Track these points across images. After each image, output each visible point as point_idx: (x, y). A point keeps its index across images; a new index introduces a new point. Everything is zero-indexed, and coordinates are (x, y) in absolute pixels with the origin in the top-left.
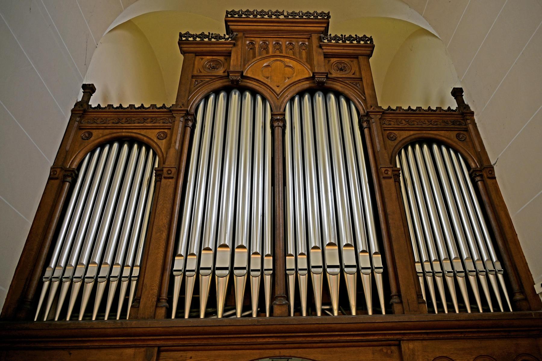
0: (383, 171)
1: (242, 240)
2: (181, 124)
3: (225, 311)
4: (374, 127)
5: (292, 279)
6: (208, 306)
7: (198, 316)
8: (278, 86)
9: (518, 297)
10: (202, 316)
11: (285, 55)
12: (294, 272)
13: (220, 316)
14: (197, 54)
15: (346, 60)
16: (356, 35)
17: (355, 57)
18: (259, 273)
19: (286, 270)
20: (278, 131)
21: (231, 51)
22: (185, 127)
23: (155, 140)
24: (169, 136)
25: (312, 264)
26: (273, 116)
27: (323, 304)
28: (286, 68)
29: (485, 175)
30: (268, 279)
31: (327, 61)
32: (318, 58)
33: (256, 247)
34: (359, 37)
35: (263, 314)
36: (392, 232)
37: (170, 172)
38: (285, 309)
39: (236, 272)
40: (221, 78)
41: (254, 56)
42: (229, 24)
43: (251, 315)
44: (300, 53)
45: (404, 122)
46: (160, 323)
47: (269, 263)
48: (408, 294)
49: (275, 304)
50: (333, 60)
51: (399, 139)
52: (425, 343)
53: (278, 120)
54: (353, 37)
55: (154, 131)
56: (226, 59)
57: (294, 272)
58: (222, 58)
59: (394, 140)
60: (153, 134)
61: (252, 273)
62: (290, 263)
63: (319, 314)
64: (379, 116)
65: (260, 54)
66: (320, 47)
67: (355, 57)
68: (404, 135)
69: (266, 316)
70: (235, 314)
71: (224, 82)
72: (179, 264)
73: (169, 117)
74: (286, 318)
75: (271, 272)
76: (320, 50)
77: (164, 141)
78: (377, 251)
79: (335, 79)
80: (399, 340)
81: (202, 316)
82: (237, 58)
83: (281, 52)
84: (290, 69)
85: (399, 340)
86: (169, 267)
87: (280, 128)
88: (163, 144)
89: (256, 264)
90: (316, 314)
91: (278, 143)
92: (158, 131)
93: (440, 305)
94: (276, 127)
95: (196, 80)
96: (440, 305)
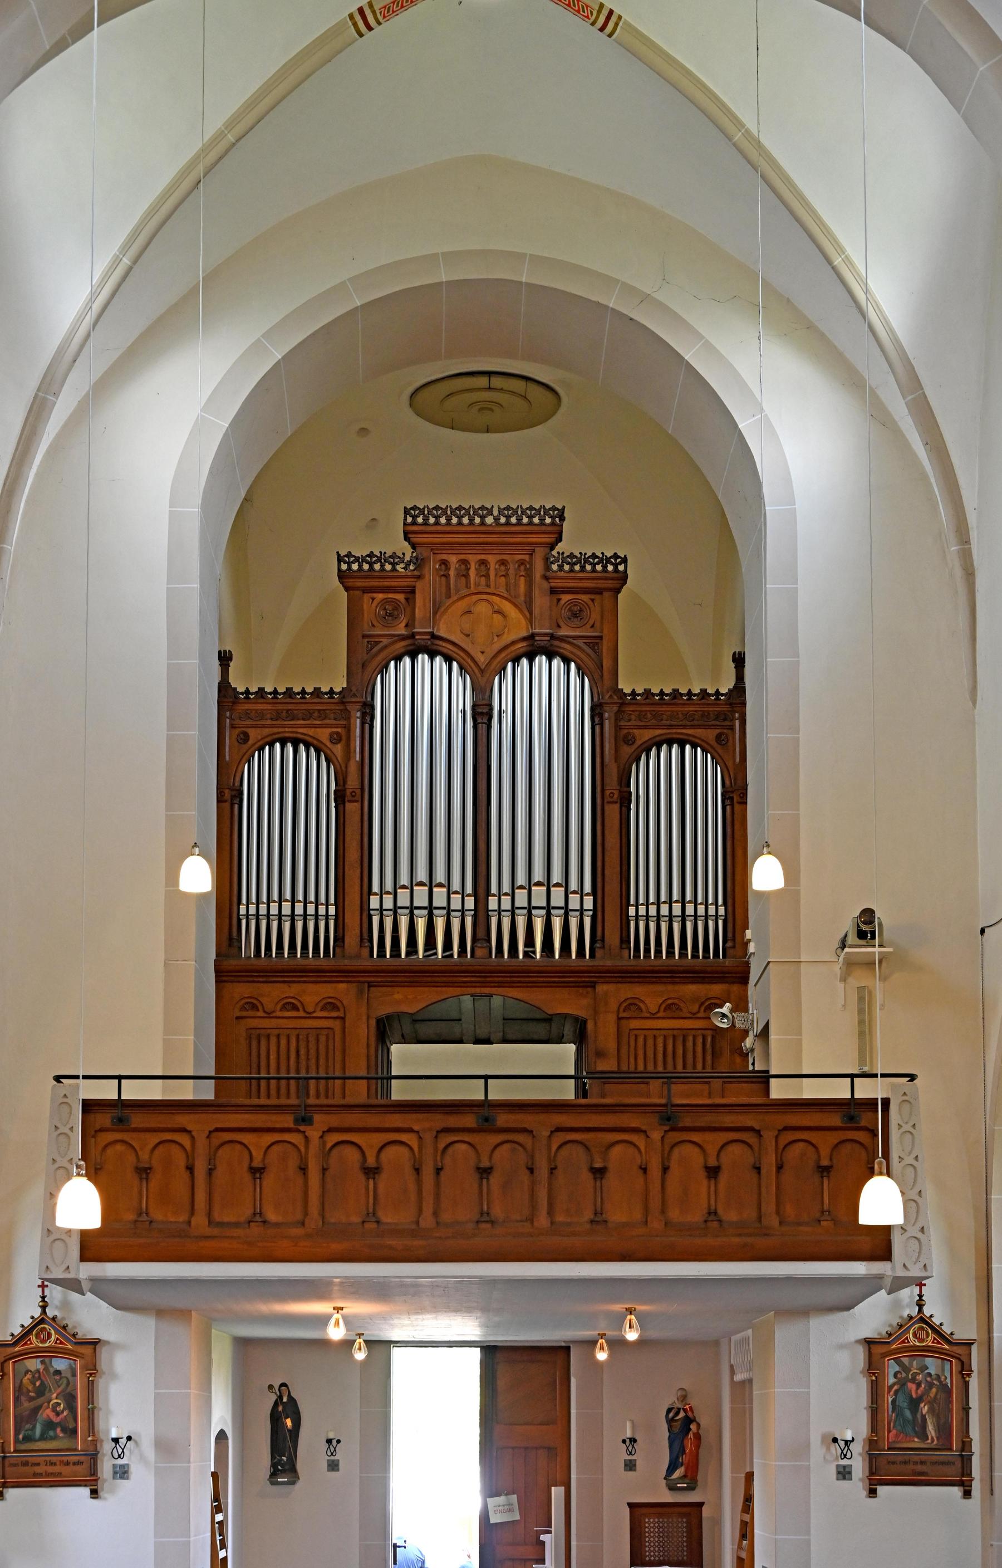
0: (608, 794)
1: (440, 877)
2: (358, 721)
3: (425, 950)
4: (607, 723)
5: (494, 921)
6: (408, 945)
7: (399, 956)
8: (483, 652)
9: (729, 944)
10: (403, 956)
11: (495, 592)
12: (496, 913)
13: (421, 957)
14: (365, 590)
15: (585, 598)
16: (603, 553)
17: (599, 592)
18: (459, 914)
19: (488, 910)
20: (482, 729)
21: (415, 587)
22: (363, 724)
23: (328, 744)
24: (344, 738)
25: (517, 905)
26: (476, 708)
27: (526, 945)
28: (495, 615)
29: (735, 800)
30: (469, 921)
31: (555, 601)
32: (541, 601)
33: (456, 885)
34: (606, 556)
35: (464, 955)
36: (607, 872)
37: (353, 794)
38: (486, 951)
39: (435, 912)
40: (403, 638)
41: (449, 596)
42: (410, 536)
43: (452, 956)
44: (516, 585)
45: (649, 715)
46: (365, 963)
47: (470, 903)
48: (612, 938)
49: (476, 946)
50: (565, 598)
51: (638, 743)
52: (620, 985)
53: (482, 713)
54: (597, 557)
55: (324, 730)
56: (407, 599)
57: (496, 913)
58: (400, 597)
59: (631, 744)
60: (323, 735)
61: (453, 914)
62: (493, 903)
63: (521, 956)
64: (615, 708)
65: (457, 591)
66: (546, 578)
67: (599, 592)
68: (647, 735)
69: (467, 956)
70: (436, 954)
71: (407, 646)
72: (374, 902)
73: (341, 710)
74: (487, 960)
75: (473, 912)
76: (546, 585)
77: (339, 746)
78: (590, 891)
79: (562, 639)
80: (595, 983)
81: (403, 956)
82: (424, 605)
83: (488, 586)
84: (500, 617)
85: (595, 983)
86: (365, 907)
87: (484, 725)
88: (338, 750)
89: (456, 902)
90: (518, 957)
91: (482, 749)
92: (329, 731)
93: (647, 950)
94: (479, 723)
95: (368, 642)
96: (647, 950)
